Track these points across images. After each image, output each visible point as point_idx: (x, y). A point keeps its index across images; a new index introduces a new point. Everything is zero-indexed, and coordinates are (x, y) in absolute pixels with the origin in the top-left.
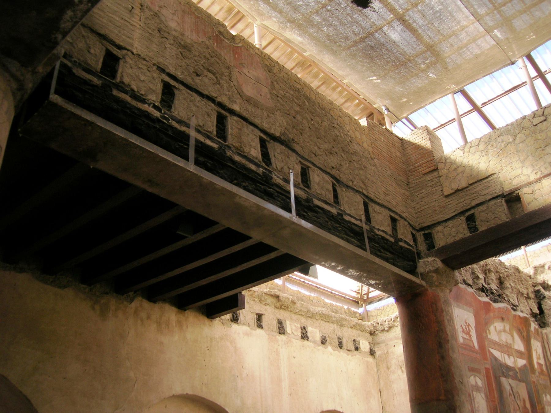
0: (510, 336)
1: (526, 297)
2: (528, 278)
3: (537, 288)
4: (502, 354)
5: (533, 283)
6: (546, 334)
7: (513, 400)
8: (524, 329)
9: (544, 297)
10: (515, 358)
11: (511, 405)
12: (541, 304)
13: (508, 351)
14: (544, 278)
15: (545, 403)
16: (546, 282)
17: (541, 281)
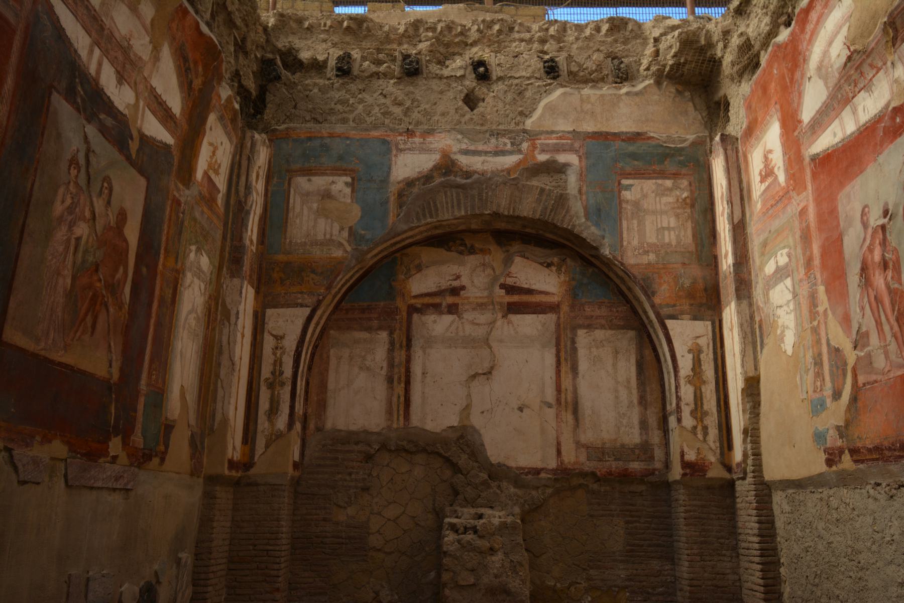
0: (148, 39)
1: (236, 44)
3: (270, 56)
4: (97, 52)
7: (76, 183)
8: (200, 69)
9: (278, 78)
10: (141, 104)
11: (61, 191)
13: (124, 67)
14: (293, 44)
15: (188, 264)
16: (293, 51)
17: (285, 46)
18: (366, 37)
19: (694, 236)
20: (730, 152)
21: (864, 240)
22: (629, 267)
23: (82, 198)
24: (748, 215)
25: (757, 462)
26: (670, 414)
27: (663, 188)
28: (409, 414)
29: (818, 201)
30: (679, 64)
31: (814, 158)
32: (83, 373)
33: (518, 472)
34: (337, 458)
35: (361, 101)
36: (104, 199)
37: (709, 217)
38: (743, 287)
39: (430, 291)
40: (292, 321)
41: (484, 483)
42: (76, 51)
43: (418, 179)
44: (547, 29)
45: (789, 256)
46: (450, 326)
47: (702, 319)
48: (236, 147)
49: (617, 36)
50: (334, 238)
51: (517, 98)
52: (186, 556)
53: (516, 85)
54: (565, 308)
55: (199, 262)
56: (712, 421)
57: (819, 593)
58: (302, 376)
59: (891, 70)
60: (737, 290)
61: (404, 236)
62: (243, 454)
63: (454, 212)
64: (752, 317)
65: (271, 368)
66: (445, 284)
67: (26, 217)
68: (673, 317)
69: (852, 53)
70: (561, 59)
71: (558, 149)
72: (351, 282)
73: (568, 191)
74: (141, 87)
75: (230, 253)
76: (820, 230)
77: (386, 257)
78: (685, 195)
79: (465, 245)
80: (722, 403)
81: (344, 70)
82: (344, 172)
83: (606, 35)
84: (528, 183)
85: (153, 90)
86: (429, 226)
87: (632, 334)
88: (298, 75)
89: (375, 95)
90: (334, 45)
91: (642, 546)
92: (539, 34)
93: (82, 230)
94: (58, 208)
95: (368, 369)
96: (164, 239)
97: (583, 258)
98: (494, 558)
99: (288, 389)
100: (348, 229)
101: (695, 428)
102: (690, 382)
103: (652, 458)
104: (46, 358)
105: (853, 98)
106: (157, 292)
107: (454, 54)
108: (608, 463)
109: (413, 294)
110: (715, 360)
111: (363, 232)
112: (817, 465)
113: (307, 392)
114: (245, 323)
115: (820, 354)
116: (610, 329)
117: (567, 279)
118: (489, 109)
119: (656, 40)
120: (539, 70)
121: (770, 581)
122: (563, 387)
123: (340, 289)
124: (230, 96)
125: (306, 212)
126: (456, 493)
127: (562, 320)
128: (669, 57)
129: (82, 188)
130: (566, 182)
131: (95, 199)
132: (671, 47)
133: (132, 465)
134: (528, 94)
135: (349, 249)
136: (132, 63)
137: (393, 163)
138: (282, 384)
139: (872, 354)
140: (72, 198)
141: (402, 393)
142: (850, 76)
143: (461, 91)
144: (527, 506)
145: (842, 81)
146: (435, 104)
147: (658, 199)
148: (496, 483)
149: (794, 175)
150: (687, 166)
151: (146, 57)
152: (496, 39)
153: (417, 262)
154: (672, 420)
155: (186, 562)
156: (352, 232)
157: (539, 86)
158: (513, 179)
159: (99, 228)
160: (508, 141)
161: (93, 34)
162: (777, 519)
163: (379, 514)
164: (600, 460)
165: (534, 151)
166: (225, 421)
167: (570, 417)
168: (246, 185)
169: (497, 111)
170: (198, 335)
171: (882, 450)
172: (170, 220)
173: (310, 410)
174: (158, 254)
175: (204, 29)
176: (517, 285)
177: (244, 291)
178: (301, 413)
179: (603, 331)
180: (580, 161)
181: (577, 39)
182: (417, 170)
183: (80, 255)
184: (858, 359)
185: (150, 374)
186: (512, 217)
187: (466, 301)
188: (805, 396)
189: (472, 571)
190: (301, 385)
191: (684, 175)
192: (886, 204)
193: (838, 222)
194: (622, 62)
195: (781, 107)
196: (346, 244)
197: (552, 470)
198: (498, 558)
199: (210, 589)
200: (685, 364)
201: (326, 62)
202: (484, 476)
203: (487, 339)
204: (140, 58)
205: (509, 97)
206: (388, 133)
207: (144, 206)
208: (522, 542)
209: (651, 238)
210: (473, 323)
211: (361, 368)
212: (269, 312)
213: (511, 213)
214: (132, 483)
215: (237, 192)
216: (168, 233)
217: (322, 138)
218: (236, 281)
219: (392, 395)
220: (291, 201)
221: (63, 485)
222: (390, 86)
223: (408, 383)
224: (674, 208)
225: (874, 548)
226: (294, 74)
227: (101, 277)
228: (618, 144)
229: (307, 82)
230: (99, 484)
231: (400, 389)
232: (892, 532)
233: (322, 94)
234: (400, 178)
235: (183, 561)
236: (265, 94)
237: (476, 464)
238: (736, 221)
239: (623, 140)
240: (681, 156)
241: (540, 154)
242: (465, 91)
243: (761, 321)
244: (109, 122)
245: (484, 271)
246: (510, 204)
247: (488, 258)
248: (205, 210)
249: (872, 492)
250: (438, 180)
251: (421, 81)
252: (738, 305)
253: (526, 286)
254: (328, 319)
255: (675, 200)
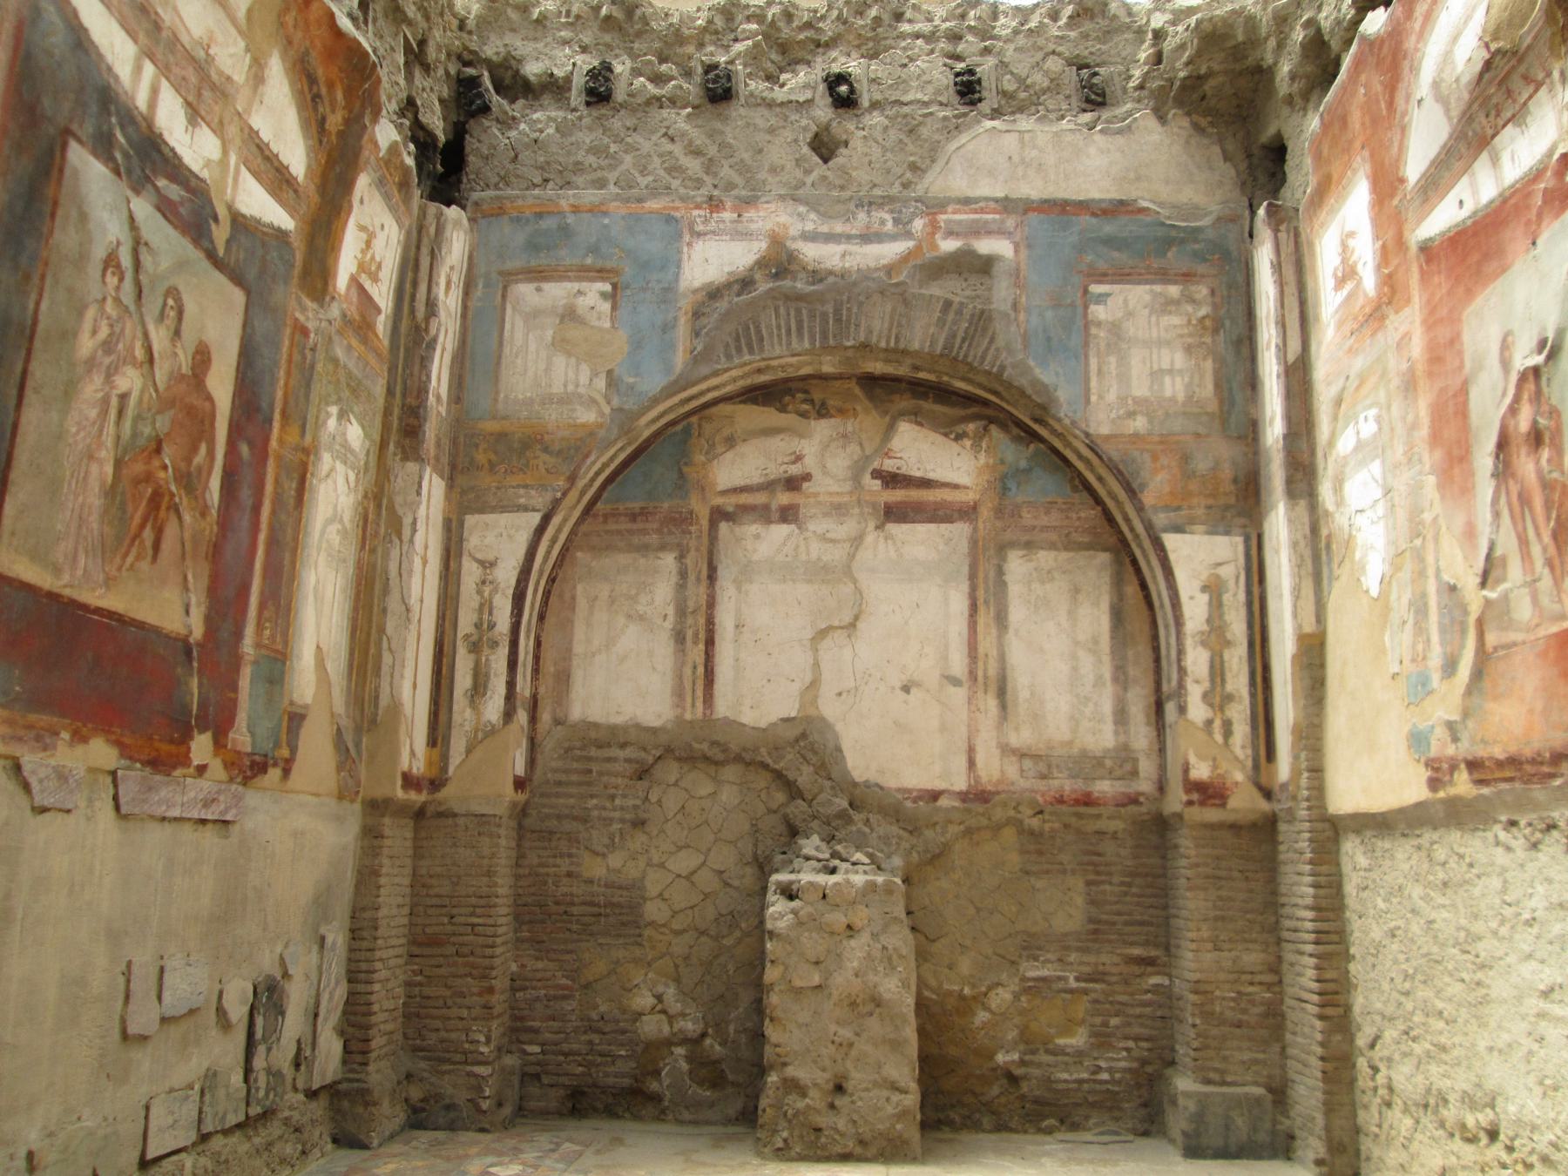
0: (242, 44)
1: (408, 49)
2: (455, 23)
3: (471, 71)
4: (149, 69)
5: (466, 48)
6: (439, 216)
7: (117, 300)
8: (340, 95)
9: (486, 109)
10: (233, 159)
11: (91, 313)
12: (466, 132)
13: (199, 95)
15: (324, 438)
16: (513, 62)
18: (639, 34)
19: (1217, 385)
20: (1283, 236)
21: (1504, 394)
22: (1099, 442)
23: (129, 325)
24: (1313, 348)
25: (1316, 783)
26: (1169, 698)
27: (1162, 300)
28: (711, 696)
29: (1430, 324)
30: (1199, 77)
31: (1426, 248)
32: (141, 625)
33: (900, 796)
34: (590, 771)
35: (630, 149)
36: (168, 328)
37: (1245, 351)
38: (1299, 476)
39: (748, 482)
40: (510, 536)
41: (843, 816)
42: (110, 69)
43: (728, 285)
44: (963, 16)
45: (1378, 420)
46: (784, 544)
47: (1227, 533)
48: (408, 233)
49: (1088, 26)
50: (581, 390)
51: (906, 140)
52: (337, 937)
53: (905, 116)
54: (985, 512)
55: (344, 434)
56: (1239, 714)
57: (1409, 1006)
58: (528, 631)
59: (1559, 87)
60: (1290, 482)
61: (703, 386)
62: (430, 763)
63: (789, 344)
64: (1315, 529)
65: (475, 617)
66: (776, 471)
67: (27, 360)
68: (1178, 529)
69: (1494, 55)
70: (986, 68)
71: (978, 230)
72: (613, 466)
73: (993, 306)
74: (232, 130)
75: (400, 419)
76: (1430, 375)
77: (673, 423)
78: (1203, 311)
79: (812, 402)
80: (1259, 680)
81: (599, 93)
82: (601, 273)
83: (1069, 26)
84: (923, 291)
85: (253, 135)
86: (747, 368)
87: (1104, 557)
88: (521, 102)
89: (654, 138)
90: (584, 49)
91: (1114, 924)
92: (948, 24)
93: (130, 380)
94: (86, 345)
95: (642, 618)
96: (280, 394)
97: (1019, 424)
98: (853, 943)
99: (503, 651)
100: (603, 376)
101: (1209, 723)
102: (1204, 644)
103: (1134, 773)
104: (74, 604)
105: (1493, 136)
106: (269, 488)
107: (798, 62)
108: (1056, 783)
109: (720, 487)
110: (1249, 604)
111: (631, 380)
112: (1410, 788)
113: (537, 658)
114: (427, 538)
115: (1424, 595)
116: (1066, 549)
117: (991, 461)
118: (855, 159)
119: (1159, 35)
120: (947, 87)
121: (1331, 987)
122: (981, 650)
123: (593, 480)
124: (396, 142)
125: (532, 347)
126: (794, 832)
127: (981, 533)
128: (1179, 65)
129: (127, 308)
130: (990, 289)
131: (151, 328)
132: (1182, 47)
133: (231, 780)
134: (925, 132)
135: (607, 410)
136: (214, 87)
137: (685, 257)
138: (494, 644)
139: (1512, 596)
140: (111, 326)
141: (700, 660)
142: (1489, 97)
143: (805, 129)
144: (915, 855)
145: (1476, 106)
146: (760, 151)
147: (1154, 319)
148: (863, 816)
149: (1390, 276)
150: (1205, 260)
151: (239, 77)
152: (870, 35)
153: (726, 432)
154: (1170, 708)
155: (334, 943)
156: (612, 381)
157: (945, 118)
158: (897, 285)
159: (161, 375)
160: (887, 217)
161: (141, 36)
162: (1346, 879)
163: (662, 865)
164: (1043, 777)
165: (933, 234)
166: (396, 707)
167: (992, 703)
168: (428, 299)
169: (870, 163)
170: (344, 561)
171: (1521, 763)
172: (290, 361)
173: (542, 690)
174: (270, 421)
175: (345, 23)
176: (903, 471)
177: (425, 484)
178: (527, 693)
179: (1053, 554)
180: (1016, 251)
181: (1016, 32)
182: (726, 269)
183: (127, 425)
184: (1488, 603)
185: (260, 626)
186: (895, 351)
187: (812, 500)
188: (1395, 668)
189: (817, 963)
190: (526, 645)
191: (1203, 276)
192: (1544, 329)
193: (1462, 362)
194: (1096, 74)
195: (1372, 155)
196: (602, 401)
197: (961, 793)
198: (864, 938)
199: (377, 987)
200: (1195, 610)
201: (568, 79)
202: (844, 803)
203: (849, 567)
204: (229, 78)
205: (893, 135)
206: (678, 204)
207: (242, 338)
208: (903, 916)
209: (1140, 389)
210: (824, 538)
211: (629, 617)
212: (471, 520)
213: (892, 344)
214: (234, 811)
215: (412, 311)
216: (286, 384)
217: (561, 213)
218: (412, 466)
219: (683, 664)
220: (508, 326)
221: (111, 813)
222: (679, 120)
223: (710, 642)
224: (1181, 336)
225: (1504, 931)
226: (513, 101)
227: (167, 462)
228: (1086, 220)
229: (535, 116)
230: (176, 813)
231: (696, 653)
232: (1533, 903)
233: (563, 135)
234: (697, 284)
235: (329, 940)
236: (463, 139)
237: (828, 784)
238: (1291, 358)
239: (1094, 214)
240: (1196, 241)
241: (945, 239)
242: (814, 128)
243: (1329, 536)
244: (174, 191)
245: (844, 447)
246: (890, 330)
247: (850, 425)
248: (354, 343)
249: (1502, 835)
250: (763, 286)
251: (737, 111)
252: (1291, 507)
253: (918, 474)
254: (573, 532)
255: (1185, 322)
